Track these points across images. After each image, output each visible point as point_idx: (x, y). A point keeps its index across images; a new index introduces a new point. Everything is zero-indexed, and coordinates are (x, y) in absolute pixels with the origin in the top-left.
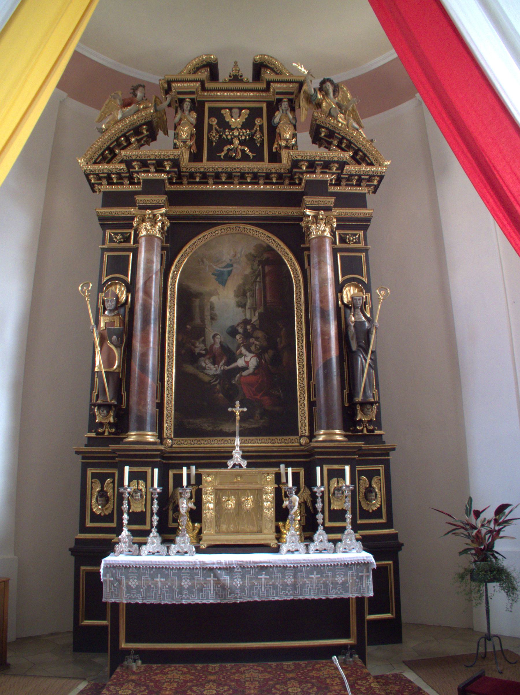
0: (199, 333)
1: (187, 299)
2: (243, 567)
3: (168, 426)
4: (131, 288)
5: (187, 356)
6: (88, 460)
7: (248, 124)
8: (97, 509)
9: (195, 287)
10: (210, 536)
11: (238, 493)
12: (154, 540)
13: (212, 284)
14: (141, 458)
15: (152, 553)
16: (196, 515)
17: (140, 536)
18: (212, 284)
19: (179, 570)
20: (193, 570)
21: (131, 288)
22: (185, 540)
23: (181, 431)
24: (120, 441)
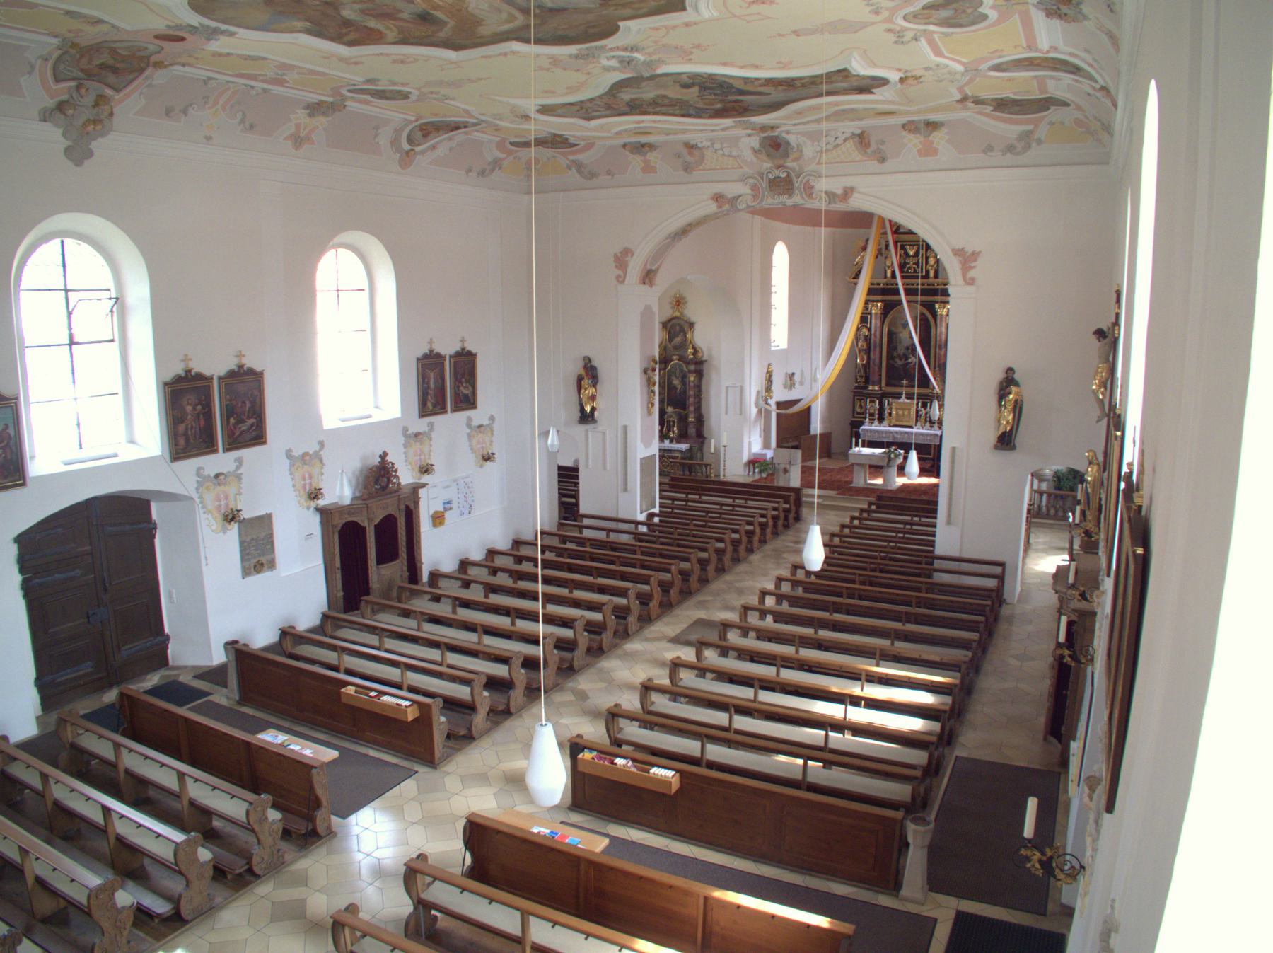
0: (895, 348)
1: (890, 334)
2: (901, 433)
3: (883, 383)
4: (869, 330)
5: (890, 357)
6: (855, 394)
7: (917, 254)
8: (859, 410)
9: (893, 329)
10: (894, 422)
11: (903, 409)
12: (876, 422)
13: (900, 329)
14: (872, 396)
15: (875, 427)
16: (890, 414)
17: (872, 421)
18: (900, 329)
19: (882, 432)
20: (887, 432)
21: (869, 330)
22: (885, 423)
23: (887, 385)
24: (866, 388)
